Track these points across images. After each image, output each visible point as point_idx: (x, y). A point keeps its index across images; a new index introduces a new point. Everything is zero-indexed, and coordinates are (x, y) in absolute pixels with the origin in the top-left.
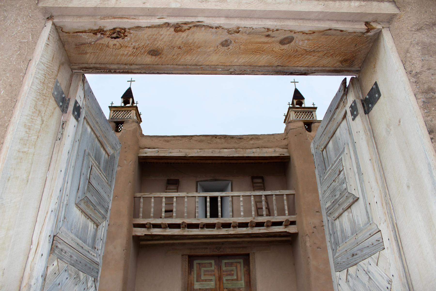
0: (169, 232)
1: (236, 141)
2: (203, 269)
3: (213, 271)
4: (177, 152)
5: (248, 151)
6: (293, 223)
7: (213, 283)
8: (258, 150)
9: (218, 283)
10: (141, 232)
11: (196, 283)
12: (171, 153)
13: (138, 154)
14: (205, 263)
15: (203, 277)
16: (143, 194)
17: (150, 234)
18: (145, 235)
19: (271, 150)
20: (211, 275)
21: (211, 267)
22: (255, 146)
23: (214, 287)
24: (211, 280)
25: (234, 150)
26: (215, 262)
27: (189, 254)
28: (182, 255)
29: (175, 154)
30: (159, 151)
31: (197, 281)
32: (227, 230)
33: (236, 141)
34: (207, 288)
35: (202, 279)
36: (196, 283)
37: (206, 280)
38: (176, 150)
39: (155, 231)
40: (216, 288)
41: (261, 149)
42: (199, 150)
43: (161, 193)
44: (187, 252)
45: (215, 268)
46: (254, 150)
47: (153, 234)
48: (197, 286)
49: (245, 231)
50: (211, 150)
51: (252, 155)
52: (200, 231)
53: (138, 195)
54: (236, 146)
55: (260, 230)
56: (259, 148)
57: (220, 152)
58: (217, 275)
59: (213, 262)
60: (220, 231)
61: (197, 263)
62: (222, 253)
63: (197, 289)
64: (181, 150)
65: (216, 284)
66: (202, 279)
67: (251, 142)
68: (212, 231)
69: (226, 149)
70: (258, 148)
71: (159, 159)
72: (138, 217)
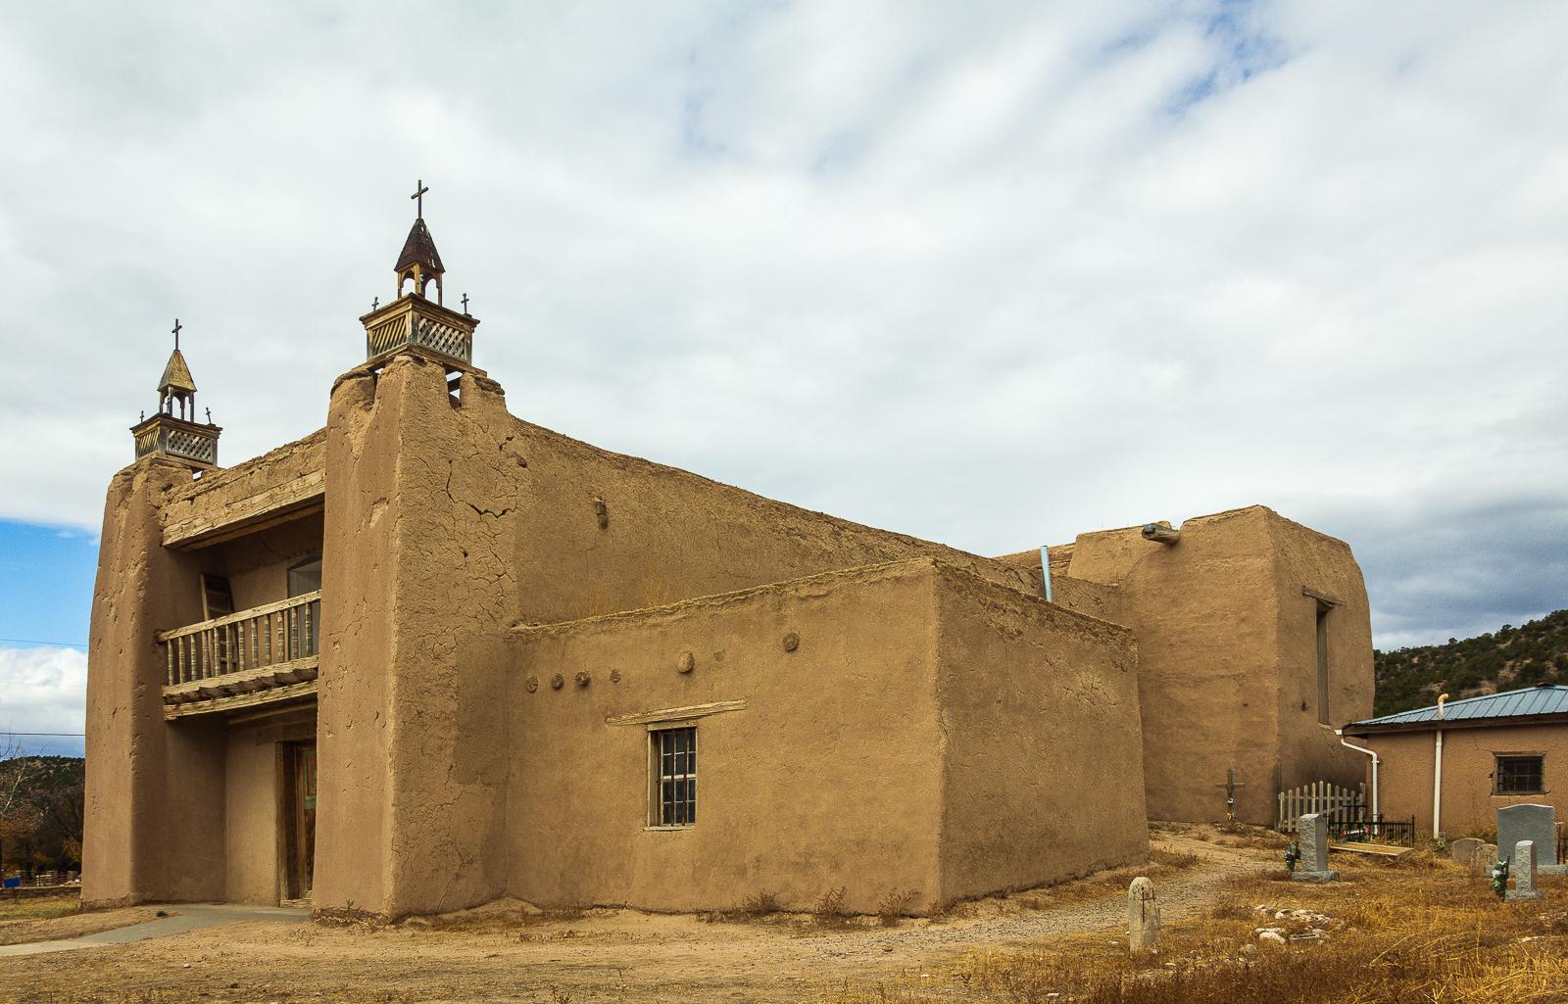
10: (171, 713)
13: (162, 542)
29: (199, 529)
68: (244, 699)
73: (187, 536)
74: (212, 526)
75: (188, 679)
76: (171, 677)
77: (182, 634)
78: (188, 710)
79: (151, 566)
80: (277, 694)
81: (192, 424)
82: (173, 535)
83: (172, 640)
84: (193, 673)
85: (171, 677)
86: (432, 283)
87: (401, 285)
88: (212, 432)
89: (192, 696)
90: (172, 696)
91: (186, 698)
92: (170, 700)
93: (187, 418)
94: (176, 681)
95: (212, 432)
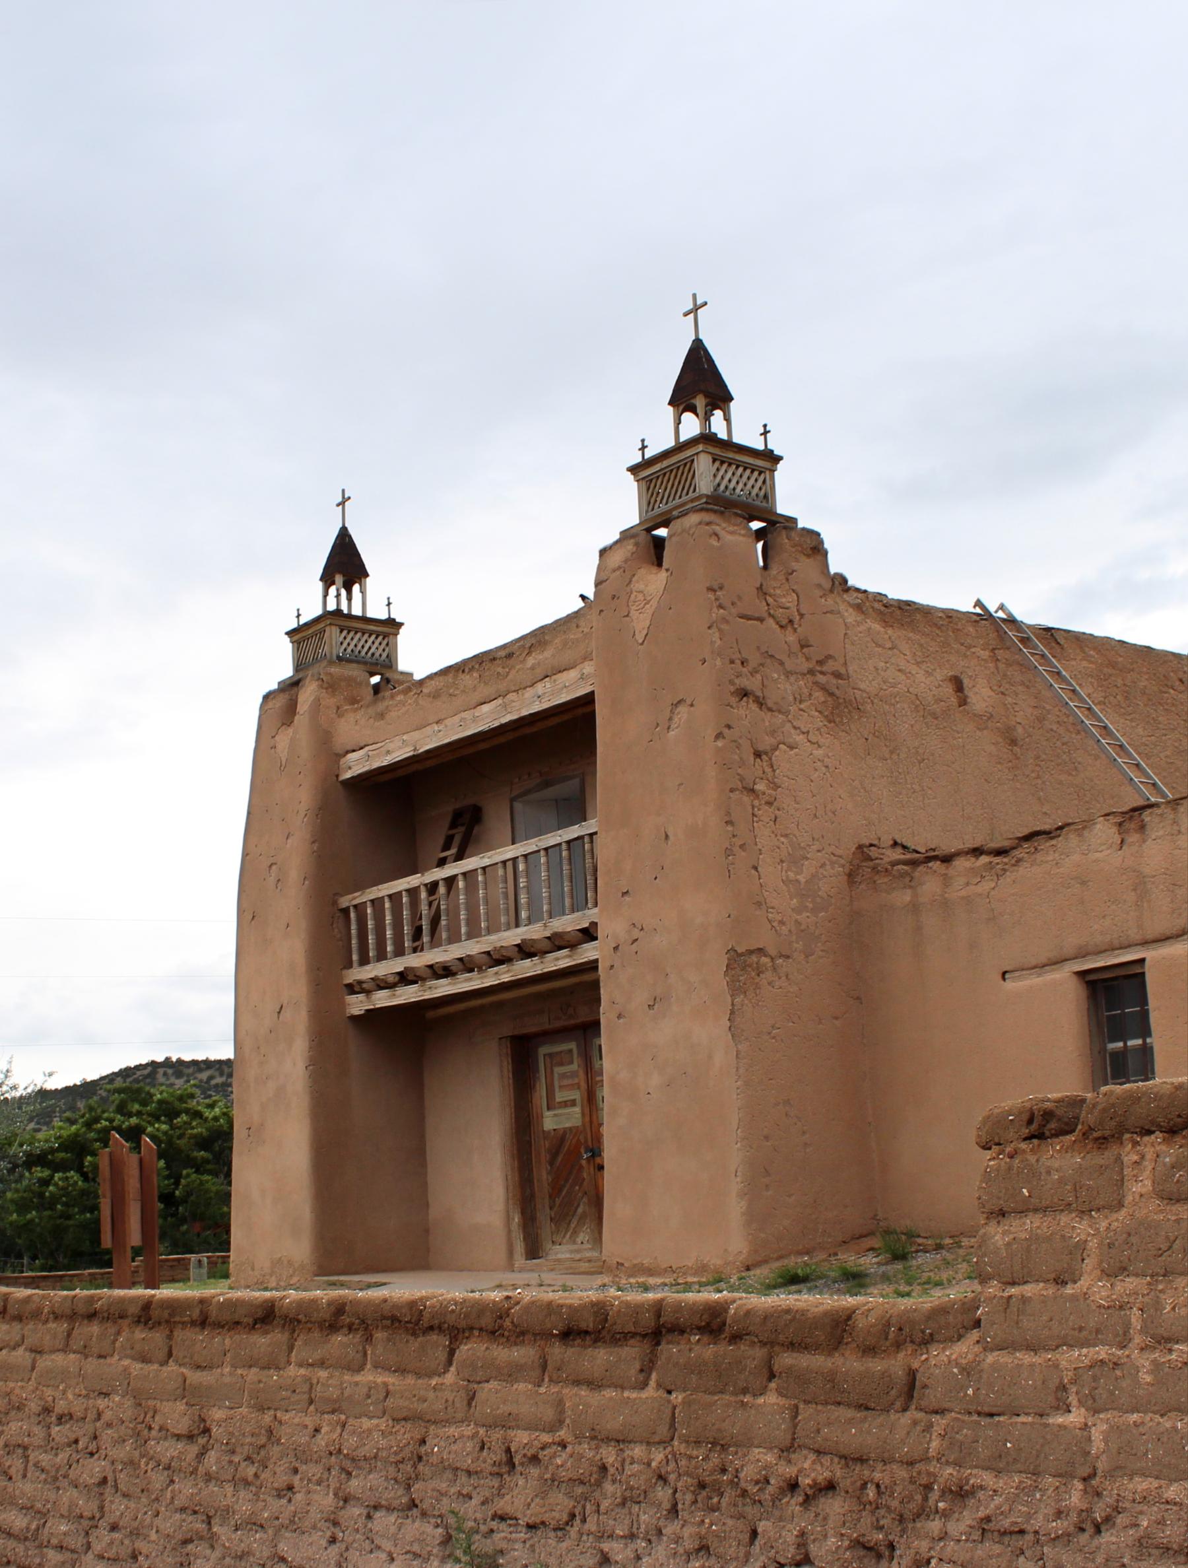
0: (401, 996)
1: (500, 670)
2: (558, 1070)
3: (574, 1074)
4: (400, 748)
5: (529, 693)
6: (588, 934)
7: (577, 1109)
8: (548, 683)
9: (587, 1111)
10: (357, 1005)
11: (547, 1114)
12: (388, 752)
13: (337, 776)
14: (561, 1052)
15: (560, 1096)
16: (350, 896)
17: (372, 1007)
18: (367, 1011)
19: (573, 674)
20: (571, 1087)
21: (572, 1062)
22: (539, 672)
23: (579, 1123)
24: (573, 1103)
25: (500, 701)
26: (578, 1046)
27: (510, 1034)
28: (500, 1038)
30: (370, 753)
31: (549, 1109)
32: (496, 973)
33: (500, 670)
34: (567, 1125)
35: (558, 1099)
36: (547, 1114)
37: (565, 1102)
38: (397, 742)
39: (380, 999)
40: (584, 1124)
41: (554, 677)
42: (436, 728)
43: (380, 887)
44: (508, 1030)
45: (579, 1066)
46: (539, 688)
47: (377, 1006)
48: (550, 1121)
49: (529, 968)
50: (457, 719)
51: (536, 708)
52: (450, 984)
53: (345, 901)
54: (502, 686)
55: (557, 959)
56: (547, 676)
57: (475, 719)
58: (583, 1085)
59: (573, 1046)
60: (485, 977)
61: (545, 1055)
62: (572, 1022)
63: (549, 1132)
64: (405, 737)
65: (583, 1114)
66: (558, 1099)
67: (531, 661)
68: (470, 980)
69: (485, 703)
70: (547, 679)
71: (383, 773)
72: (349, 965)
73: (376, 764)
74: (415, 750)
75: (382, 956)
76: (355, 957)
77: (372, 897)
78: (383, 999)
79: (323, 809)
80: (561, 960)
81: (364, 619)
82: (356, 765)
83: (355, 906)
84: (389, 948)
85: (355, 957)
86: (718, 414)
87: (678, 422)
88: (392, 626)
89: (391, 979)
90: (360, 982)
91: (381, 984)
92: (352, 989)
93: (357, 611)
94: (364, 961)
95: (392, 626)
